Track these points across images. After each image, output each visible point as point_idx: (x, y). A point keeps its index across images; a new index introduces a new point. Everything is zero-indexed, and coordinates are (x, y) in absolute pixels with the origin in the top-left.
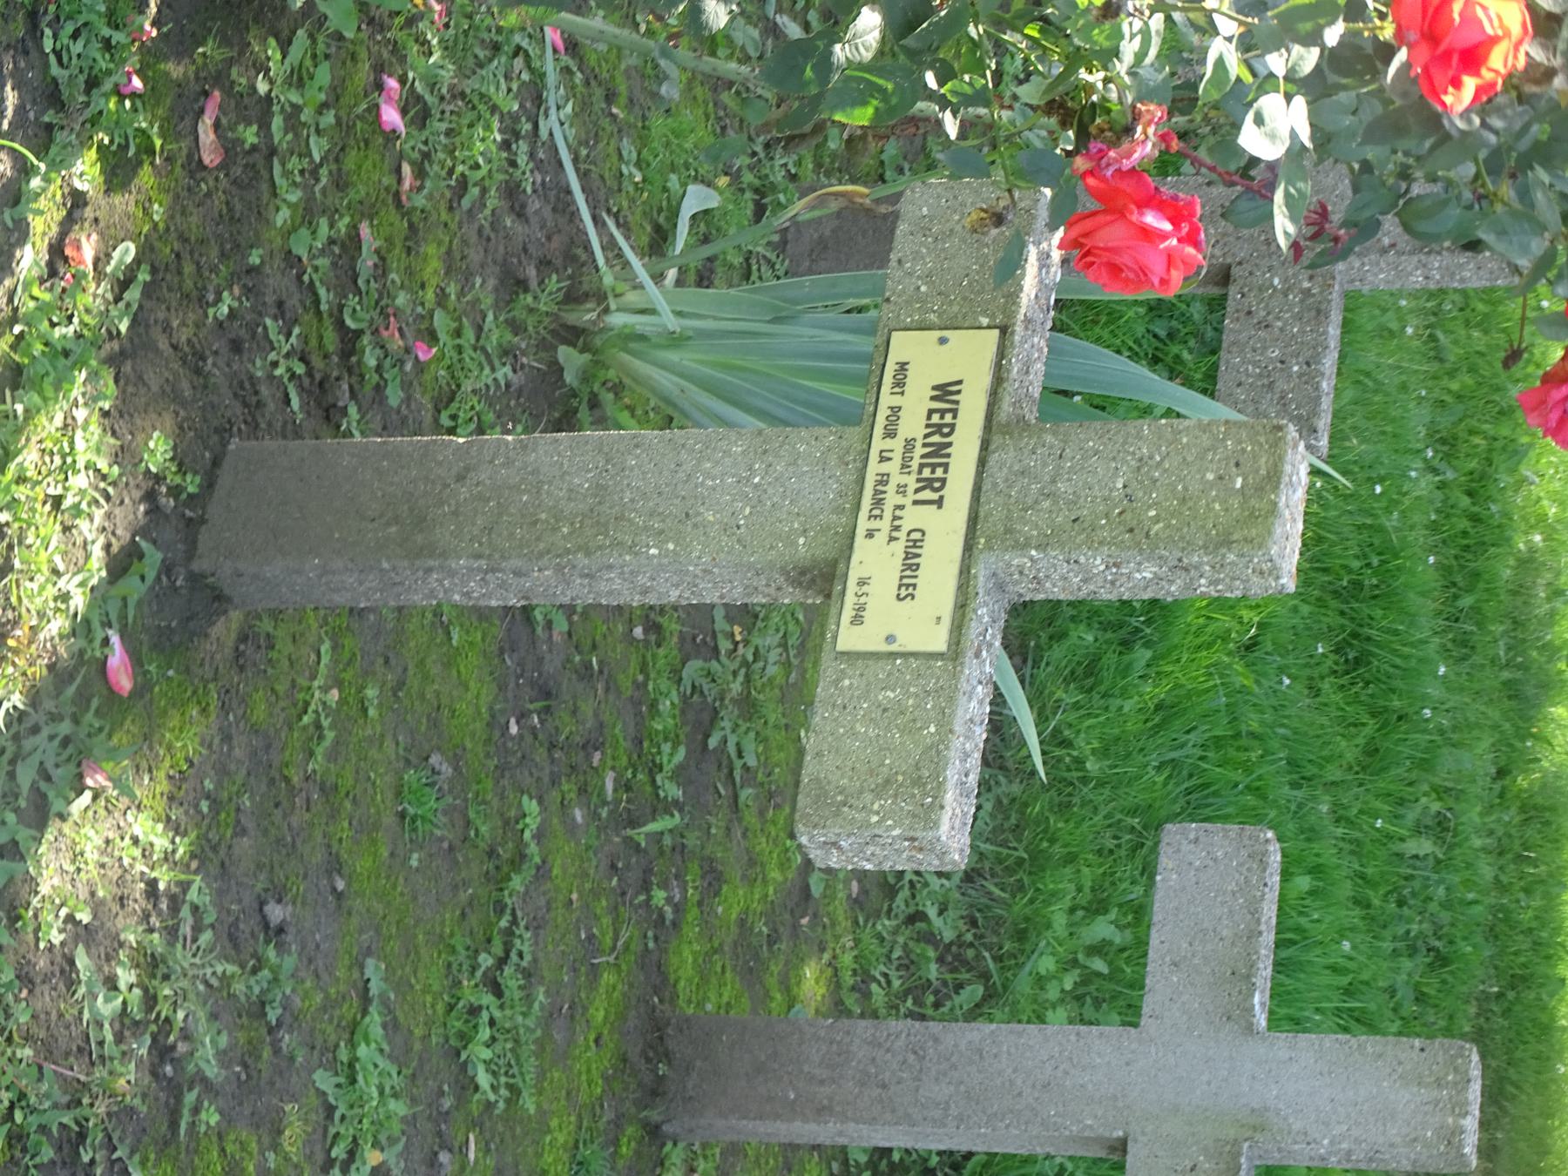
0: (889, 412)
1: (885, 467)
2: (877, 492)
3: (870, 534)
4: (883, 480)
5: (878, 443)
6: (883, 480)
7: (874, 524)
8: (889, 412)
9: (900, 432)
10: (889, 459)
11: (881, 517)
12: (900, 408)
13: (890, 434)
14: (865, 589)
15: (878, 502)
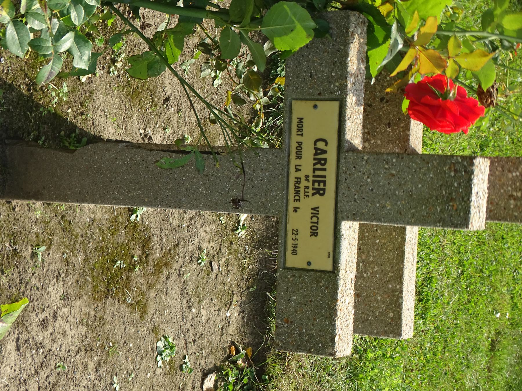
0: (297, 145)
1: (298, 174)
2: (296, 187)
3: (296, 210)
4: (298, 181)
5: (294, 162)
6: (298, 181)
7: (297, 204)
8: (297, 145)
9: (303, 156)
10: (300, 170)
11: (299, 200)
12: (302, 143)
13: (299, 157)
14: (297, 237)
15: (297, 193)
